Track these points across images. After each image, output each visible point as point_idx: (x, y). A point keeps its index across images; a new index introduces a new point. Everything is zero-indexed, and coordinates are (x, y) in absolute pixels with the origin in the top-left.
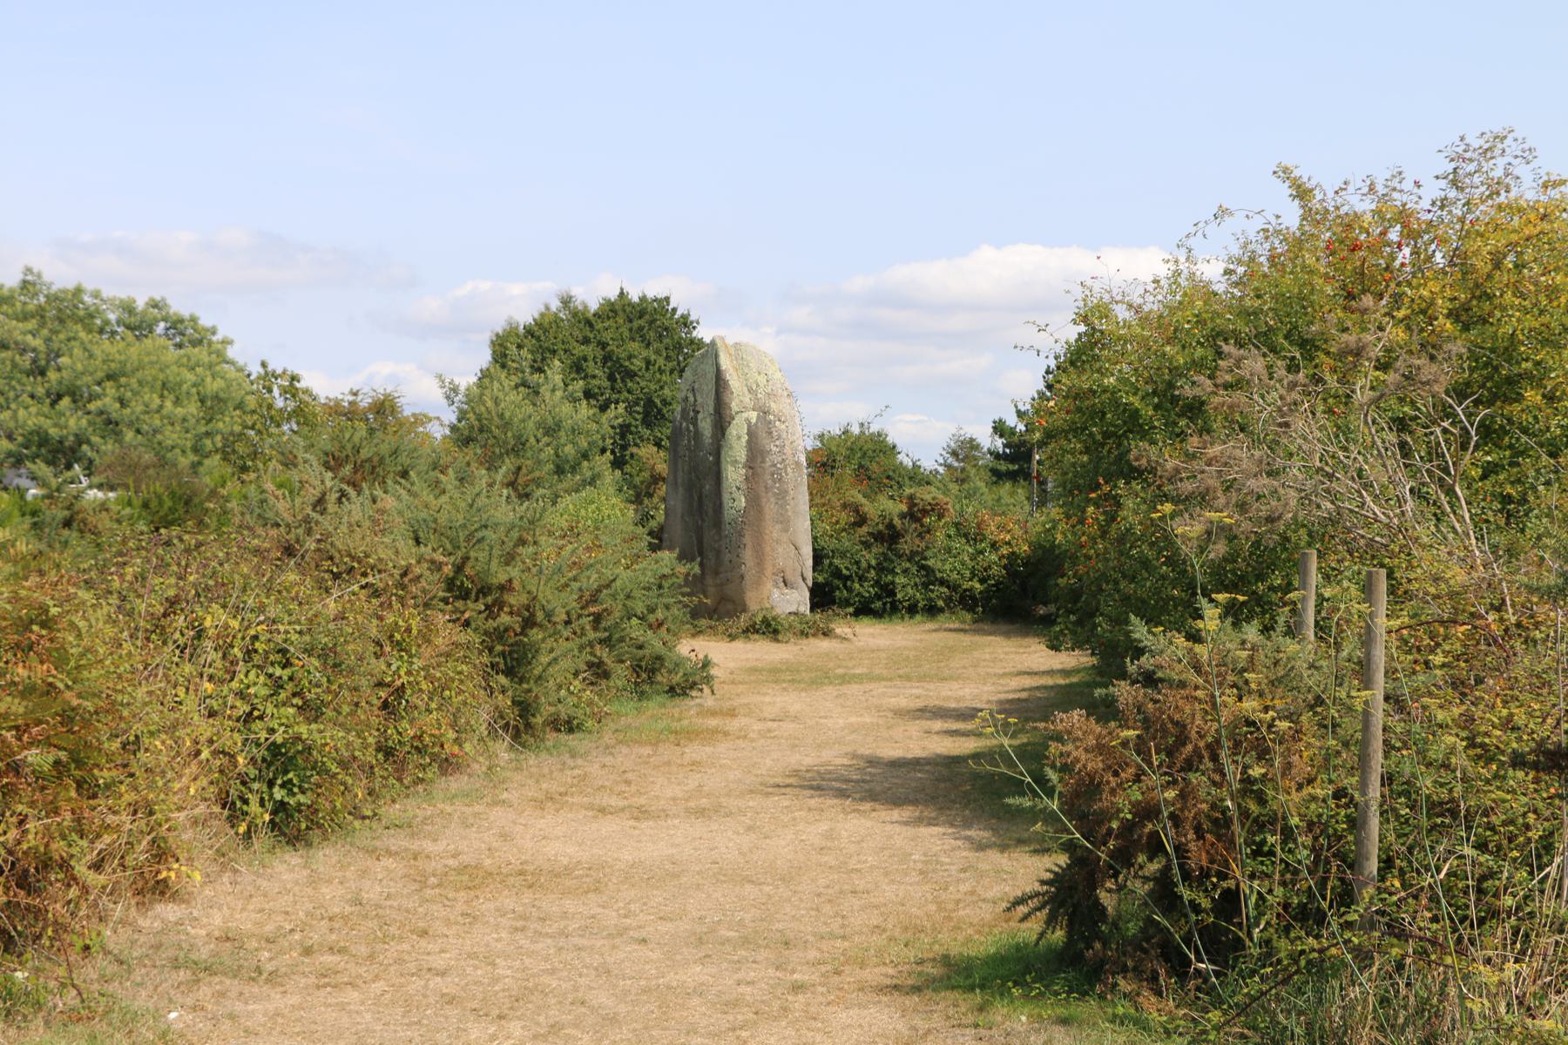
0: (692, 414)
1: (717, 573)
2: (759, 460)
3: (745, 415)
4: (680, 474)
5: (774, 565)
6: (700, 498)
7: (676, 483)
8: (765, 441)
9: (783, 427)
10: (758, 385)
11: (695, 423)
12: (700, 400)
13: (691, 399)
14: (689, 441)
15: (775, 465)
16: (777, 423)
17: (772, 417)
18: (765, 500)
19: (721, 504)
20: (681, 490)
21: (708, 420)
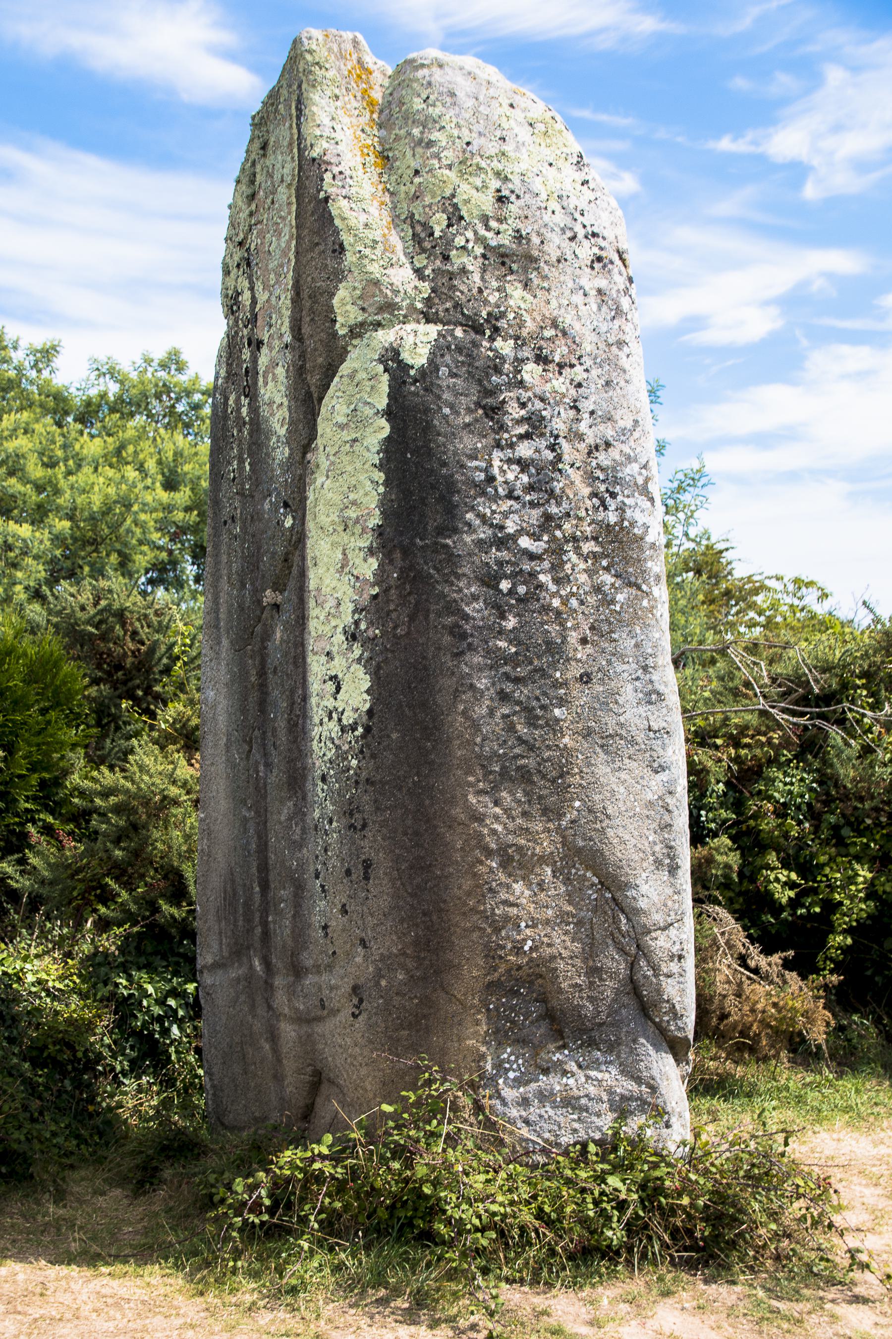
0: (246, 354)
1: (298, 971)
2: (434, 521)
3: (385, 337)
4: (225, 586)
5: (491, 954)
6: (262, 673)
7: (217, 627)
8: (468, 442)
9: (560, 384)
10: (455, 217)
11: (251, 392)
12: (262, 297)
13: (246, 298)
14: (241, 461)
15: (504, 541)
16: (531, 372)
17: (505, 347)
18: (448, 683)
19: (305, 698)
20: (225, 642)
21: (280, 371)
